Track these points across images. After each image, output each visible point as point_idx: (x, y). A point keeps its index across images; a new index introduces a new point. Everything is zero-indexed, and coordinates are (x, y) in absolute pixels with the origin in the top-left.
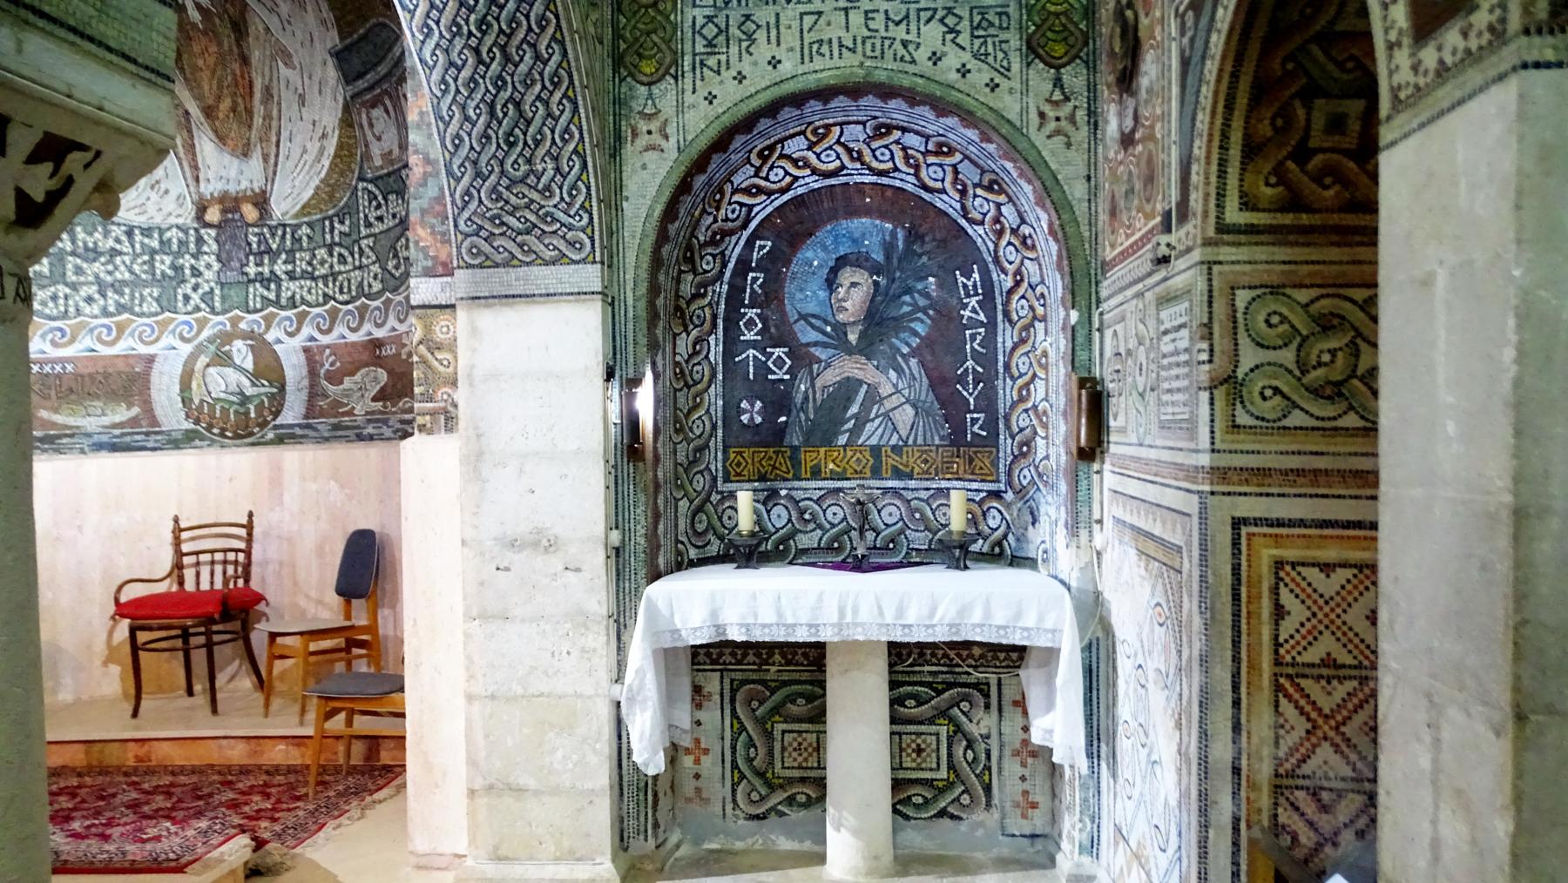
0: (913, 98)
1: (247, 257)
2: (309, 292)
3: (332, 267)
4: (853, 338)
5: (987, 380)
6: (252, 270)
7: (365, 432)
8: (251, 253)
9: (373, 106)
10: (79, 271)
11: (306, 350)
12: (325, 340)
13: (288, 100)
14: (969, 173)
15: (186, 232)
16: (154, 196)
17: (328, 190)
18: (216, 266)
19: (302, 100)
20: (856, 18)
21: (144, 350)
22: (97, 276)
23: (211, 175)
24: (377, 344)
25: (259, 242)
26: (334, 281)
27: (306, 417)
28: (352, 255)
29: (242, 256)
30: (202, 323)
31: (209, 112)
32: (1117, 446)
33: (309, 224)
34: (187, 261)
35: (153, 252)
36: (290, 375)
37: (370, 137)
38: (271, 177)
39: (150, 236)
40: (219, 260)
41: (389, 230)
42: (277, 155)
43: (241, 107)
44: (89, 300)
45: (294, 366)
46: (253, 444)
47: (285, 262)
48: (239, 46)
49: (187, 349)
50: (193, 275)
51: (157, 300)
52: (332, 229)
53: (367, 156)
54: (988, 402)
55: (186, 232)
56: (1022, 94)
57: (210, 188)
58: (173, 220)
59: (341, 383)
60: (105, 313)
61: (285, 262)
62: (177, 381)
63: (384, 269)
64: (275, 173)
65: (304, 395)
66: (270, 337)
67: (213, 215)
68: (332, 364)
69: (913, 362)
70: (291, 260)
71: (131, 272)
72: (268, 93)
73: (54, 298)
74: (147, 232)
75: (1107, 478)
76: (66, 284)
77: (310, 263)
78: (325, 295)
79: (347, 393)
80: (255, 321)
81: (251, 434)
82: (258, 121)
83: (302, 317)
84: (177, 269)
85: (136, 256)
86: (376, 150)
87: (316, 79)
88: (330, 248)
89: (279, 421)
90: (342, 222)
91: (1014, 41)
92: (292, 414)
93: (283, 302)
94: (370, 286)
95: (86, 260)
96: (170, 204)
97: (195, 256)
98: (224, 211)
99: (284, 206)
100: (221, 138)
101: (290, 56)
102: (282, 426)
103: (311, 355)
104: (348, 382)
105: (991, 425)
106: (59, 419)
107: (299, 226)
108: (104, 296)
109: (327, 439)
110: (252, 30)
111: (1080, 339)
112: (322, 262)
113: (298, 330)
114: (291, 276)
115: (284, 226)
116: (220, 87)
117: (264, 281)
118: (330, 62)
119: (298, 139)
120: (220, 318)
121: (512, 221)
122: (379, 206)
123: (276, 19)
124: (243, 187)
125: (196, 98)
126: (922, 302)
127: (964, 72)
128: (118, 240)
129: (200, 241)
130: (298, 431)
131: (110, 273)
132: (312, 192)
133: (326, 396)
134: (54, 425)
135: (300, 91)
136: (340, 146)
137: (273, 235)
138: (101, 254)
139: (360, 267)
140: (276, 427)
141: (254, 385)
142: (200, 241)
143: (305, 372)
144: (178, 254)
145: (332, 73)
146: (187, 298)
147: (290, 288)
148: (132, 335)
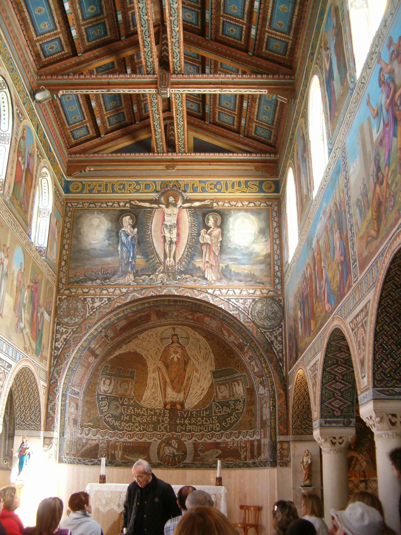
1: (177, 418)
2: (195, 428)
3: (203, 422)
4: (352, 447)
6: (178, 422)
7: (213, 466)
8: (178, 417)
9: (221, 385)
10: (135, 419)
11: (194, 444)
12: (200, 441)
13: (194, 380)
15: (161, 411)
16: (154, 401)
17: (203, 403)
18: (168, 420)
19: (199, 381)
21: (148, 441)
22: (139, 421)
23: (169, 396)
24: (219, 443)
25: (181, 415)
26: (203, 427)
27: (193, 461)
28: (209, 420)
29: (175, 417)
30: (165, 434)
31: (172, 382)
33: (197, 412)
34: (161, 418)
35: (152, 415)
36: (188, 450)
37: (218, 391)
38: (185, 398)
39: (152, 411)
40: (169, 418)
41: (223, 415)
42: (188, 393)
43: (180, 381)
44: (137, 427)
45: (190, 448)
46: (176, 468)
47: (188, 420)
48: (185, 367)
49: (160, 441)
50: (162, 422)
51: (152, 428)
52: (203, 413)
53: (217, 396)
55: (161, 411)
57: (168, 400)
58: (158, 407)
59: (204, 452)
60: (140, 431)
61: (188, 420)
62: (156, 449)
63: (221, 424)
64: (187, 397)
65: (192, 455)
66: (183, 439)
67: (168, 407)
68: (202, 448)
69: (366, 452)
70: (190, 420)
71: (146, 419)
72: (189, 378)
73: (129, 426)
74: (151, 410)
76: (132, 423)
77: (195, 421)
78: (200, 430)
79: (206, 456)
80: (179, 435)
81: (176, 465)
82: (185, 384)
83: (192, 435)
84: (158, 420)
85: (148, 416)
86: (220, 395)
87: (204, 376)
88: (202, 418)
89: (184, 462)
90: (206, 411)
92: (188, 460)
93: (187, 430)
94: (216, 429)
95: (136, 417)
96: (157, 403)
97: (163, 417)
98: (171, 406)
99: (189, 406)
100: (174, 388)
101: (198, 370)
102: (185, 463)
103: (195, 445)
104: (207, 453)
106: (128, 458)
107: (193, 412)
108: (140, 426)
109: (199, 467)
110: (189, 364)
112: (200, 421)
113: (191, 438)
114: (190, 424)
115: (188, 411)
116: (176, 376)
117: (182, 425)
118: (210, 373)
119: (195, 390)
120: (168, 434)
121: (303, 426)
122: (219, 409)
123: (197, 362)
124: (178, 400)
125: (169, 378)
126: (367, 439)
128: (144, 412)
129: (164, 413)
130: (190, 465)
131: (142, 420)
132: (197, 403)
133: (200, 456)
134: (127, 459)
135: (199, 378)
136: (208, 393)
137: (185, 413)
138: (140, 415)
139: (212, 424)
140: (183, 463)
141: (177, 452)
142: (164, 413)
143: (193, 449)
144: (159, 416)
145: (210, 375)
146: (160, 428)
147: (189, 427)
148: (146, 437)
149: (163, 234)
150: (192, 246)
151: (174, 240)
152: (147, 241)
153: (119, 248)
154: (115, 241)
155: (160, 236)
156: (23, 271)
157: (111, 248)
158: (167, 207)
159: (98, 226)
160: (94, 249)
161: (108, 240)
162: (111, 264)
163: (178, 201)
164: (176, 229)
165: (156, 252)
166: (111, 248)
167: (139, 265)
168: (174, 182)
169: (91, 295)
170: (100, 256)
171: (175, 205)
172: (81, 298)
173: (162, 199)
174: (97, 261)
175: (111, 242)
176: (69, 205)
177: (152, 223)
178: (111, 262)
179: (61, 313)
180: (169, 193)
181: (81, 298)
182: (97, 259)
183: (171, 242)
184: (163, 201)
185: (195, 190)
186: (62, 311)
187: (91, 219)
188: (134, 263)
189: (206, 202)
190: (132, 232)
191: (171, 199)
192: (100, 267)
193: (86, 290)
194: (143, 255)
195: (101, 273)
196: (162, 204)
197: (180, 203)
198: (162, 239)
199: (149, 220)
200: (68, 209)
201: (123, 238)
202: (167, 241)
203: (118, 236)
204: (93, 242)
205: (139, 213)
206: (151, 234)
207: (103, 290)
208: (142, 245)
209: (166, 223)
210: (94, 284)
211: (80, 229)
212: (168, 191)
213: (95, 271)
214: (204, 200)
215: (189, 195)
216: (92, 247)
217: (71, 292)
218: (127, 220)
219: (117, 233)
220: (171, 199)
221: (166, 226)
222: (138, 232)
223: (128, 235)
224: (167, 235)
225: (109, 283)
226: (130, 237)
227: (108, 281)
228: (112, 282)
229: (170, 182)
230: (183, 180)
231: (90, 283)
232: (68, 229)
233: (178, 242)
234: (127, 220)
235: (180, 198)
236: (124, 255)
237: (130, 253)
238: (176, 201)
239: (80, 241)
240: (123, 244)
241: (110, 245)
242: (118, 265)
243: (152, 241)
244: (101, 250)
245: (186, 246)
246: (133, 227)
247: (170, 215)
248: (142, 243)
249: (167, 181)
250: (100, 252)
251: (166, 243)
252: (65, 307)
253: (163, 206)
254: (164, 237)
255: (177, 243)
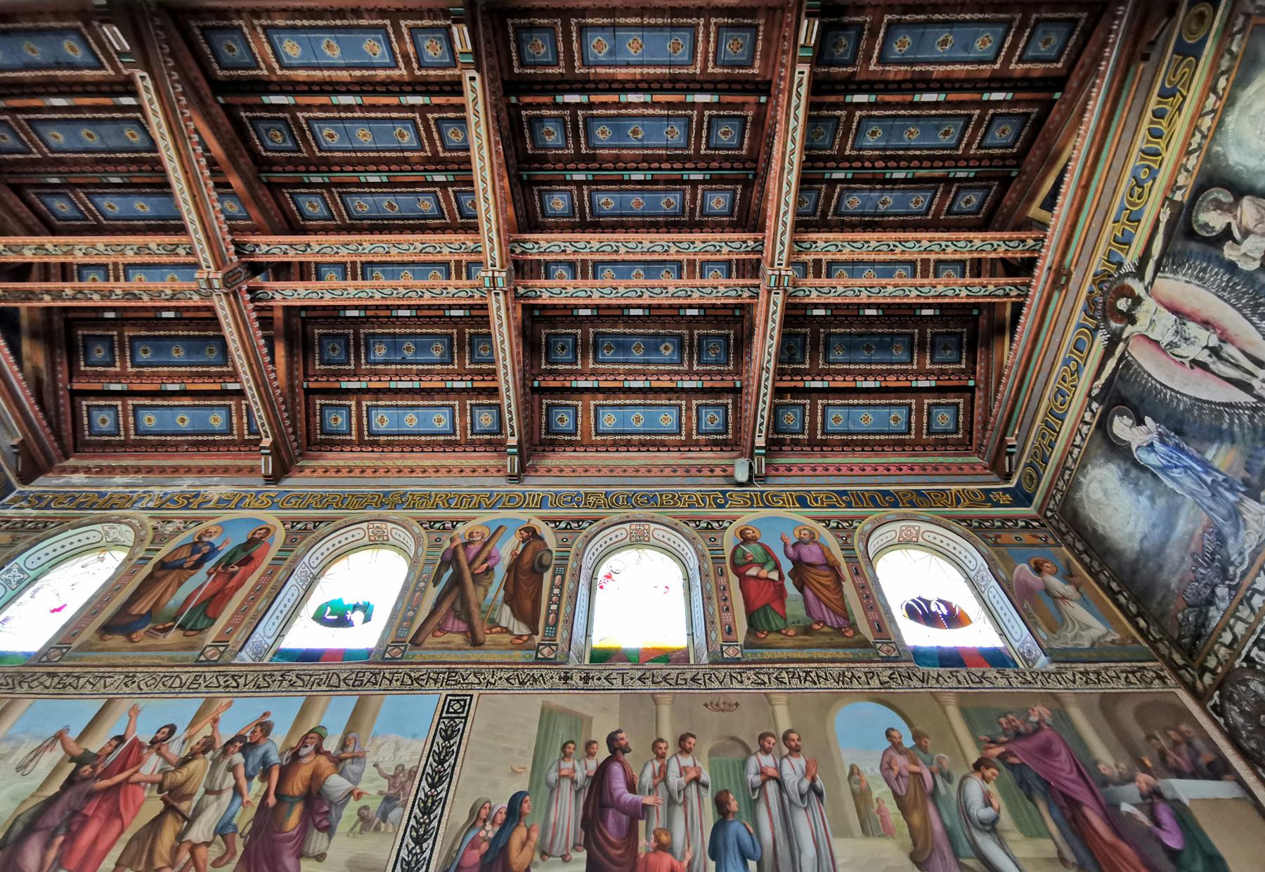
149: (1186, 362)
150: (1254, 298)
151: (1214, 341)
152: (1186, 410)
153: (1170, 485)
154: (1151, 482)
155: (1186, 371)
156: (908, 742)
157: (1161, 502)
158: (1133, 321)
159: (1105, 492)
160: (1145, 537)
161: (1140, 493)
162: (1195, 530)
163: (1132, 291)
164: (1190, 324)
165: (1220, 404)
166: (1161, 502)
167: (1231, 468)
168: (1094, 282)
169: (1245, 639)
170: (1168, 538)
171: (1137, 301)
172: (1241, 667)
173: (1114, 325)
174: (1173, 553)
175: (1148, 493)
176: (1049, 514)
177: (1149, 375)
178: (1191, 526)
179: (1254, 745)
180: (1112, 306)
181: (1241, 667)
182: (1168, 550)
183: (1215, 352)
184: (1119, 325)
185: (1124, 242)
186: (1248, 738)
187: (1088, 497)
188: (1221, 478)
189: (1164, 218)
190: (1149, 432)
191: (1123, 304)
192: (1188, 559)
193: (1227, 637)
194: (1212, 441)
195: (1205, 568)
196: (1122, 330)
197: (1138, 287)
198: (1198, 372)
199: (1143, 378)
200: (1054, 523)
201: (1152, 462)
202: (1209, 360)
203: (1143, 469)
204: (1130, 528)
205: (1119, 392)
206: (1172, 390)
207: (1249, 599)
208: (1186, 428)
209: (1164, 343)
210: (1223, 605)
211: (1095, 531)
212: (1104, 303)
213: (1191, 576)
214: (1157, 221)
215: (1130, 259)
216: (1138, 536)
217: (1213, 672)
218: (1122, 427)
219: (1136, 464)
220: (1123, 304)
221: (1171, 344)
222: (1154, 420)
223: (1151, 445)
224: (1195, 352)
225: (1239, 572)
226: (1157, 445)
227: (1231, 569)
228: (1241, 564)
229: (1091, 292)
230: (1097, 265)
231: (1215, 615)
232: (1085, 551)
233: (1222, 334)
234: (1122, 427)
235: (1129, 282)
236: (1188, 482)
237: (1190, 468)
238: (1129, 293)
239: (1117, 551)
240: (1164, 469)
241: (1152, 499)
242: (1204, 515)
243: (1190, 397)
244: (1154, 525)
245: (1245, 316)
246: (1140, 422)
247: (1152, 322)
248: (1186, 425)
249: (1087, 298)
250: (1158, 531)
251: (1212, 366)
252: (1241, 720)
253: (1129, 330)
254: (1195, 363)
255: (1224, 339)
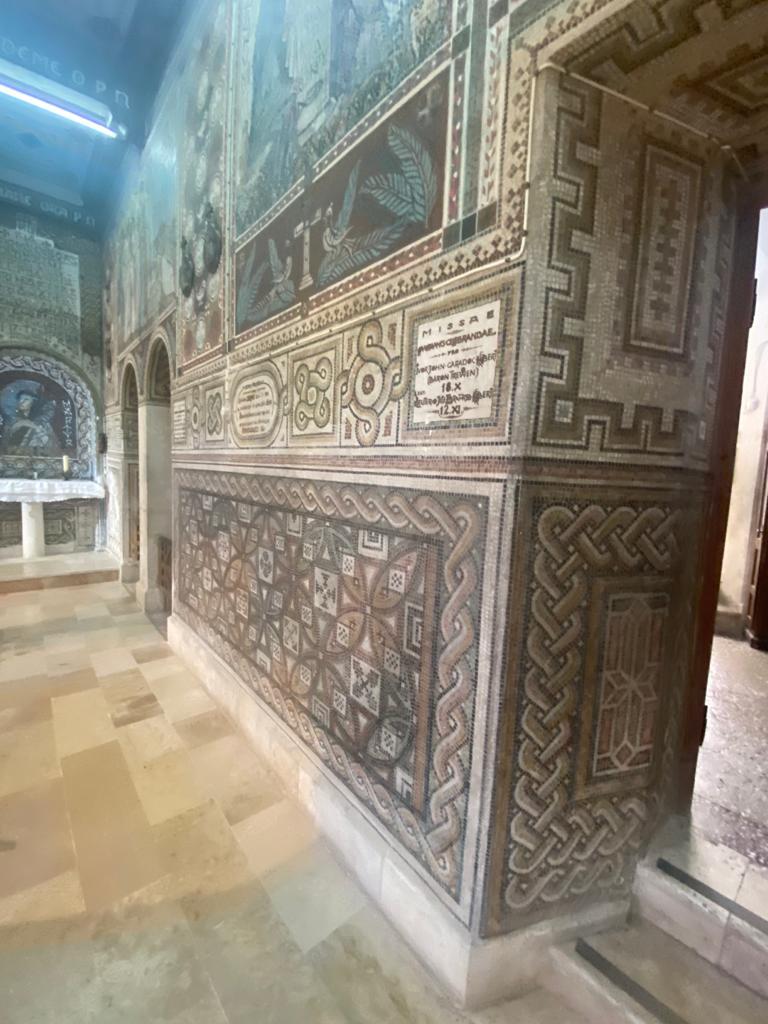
0: (48, 354)
5: (73, 430)
14: (67, 377)
20: (30, 330)
32: (109, 450)
54: (73, 437)
56: (83, 360)
75: (108, 458)
91: (80, 347)
105: (74, 442)
111: (100, 424)
127: (64, 351)
